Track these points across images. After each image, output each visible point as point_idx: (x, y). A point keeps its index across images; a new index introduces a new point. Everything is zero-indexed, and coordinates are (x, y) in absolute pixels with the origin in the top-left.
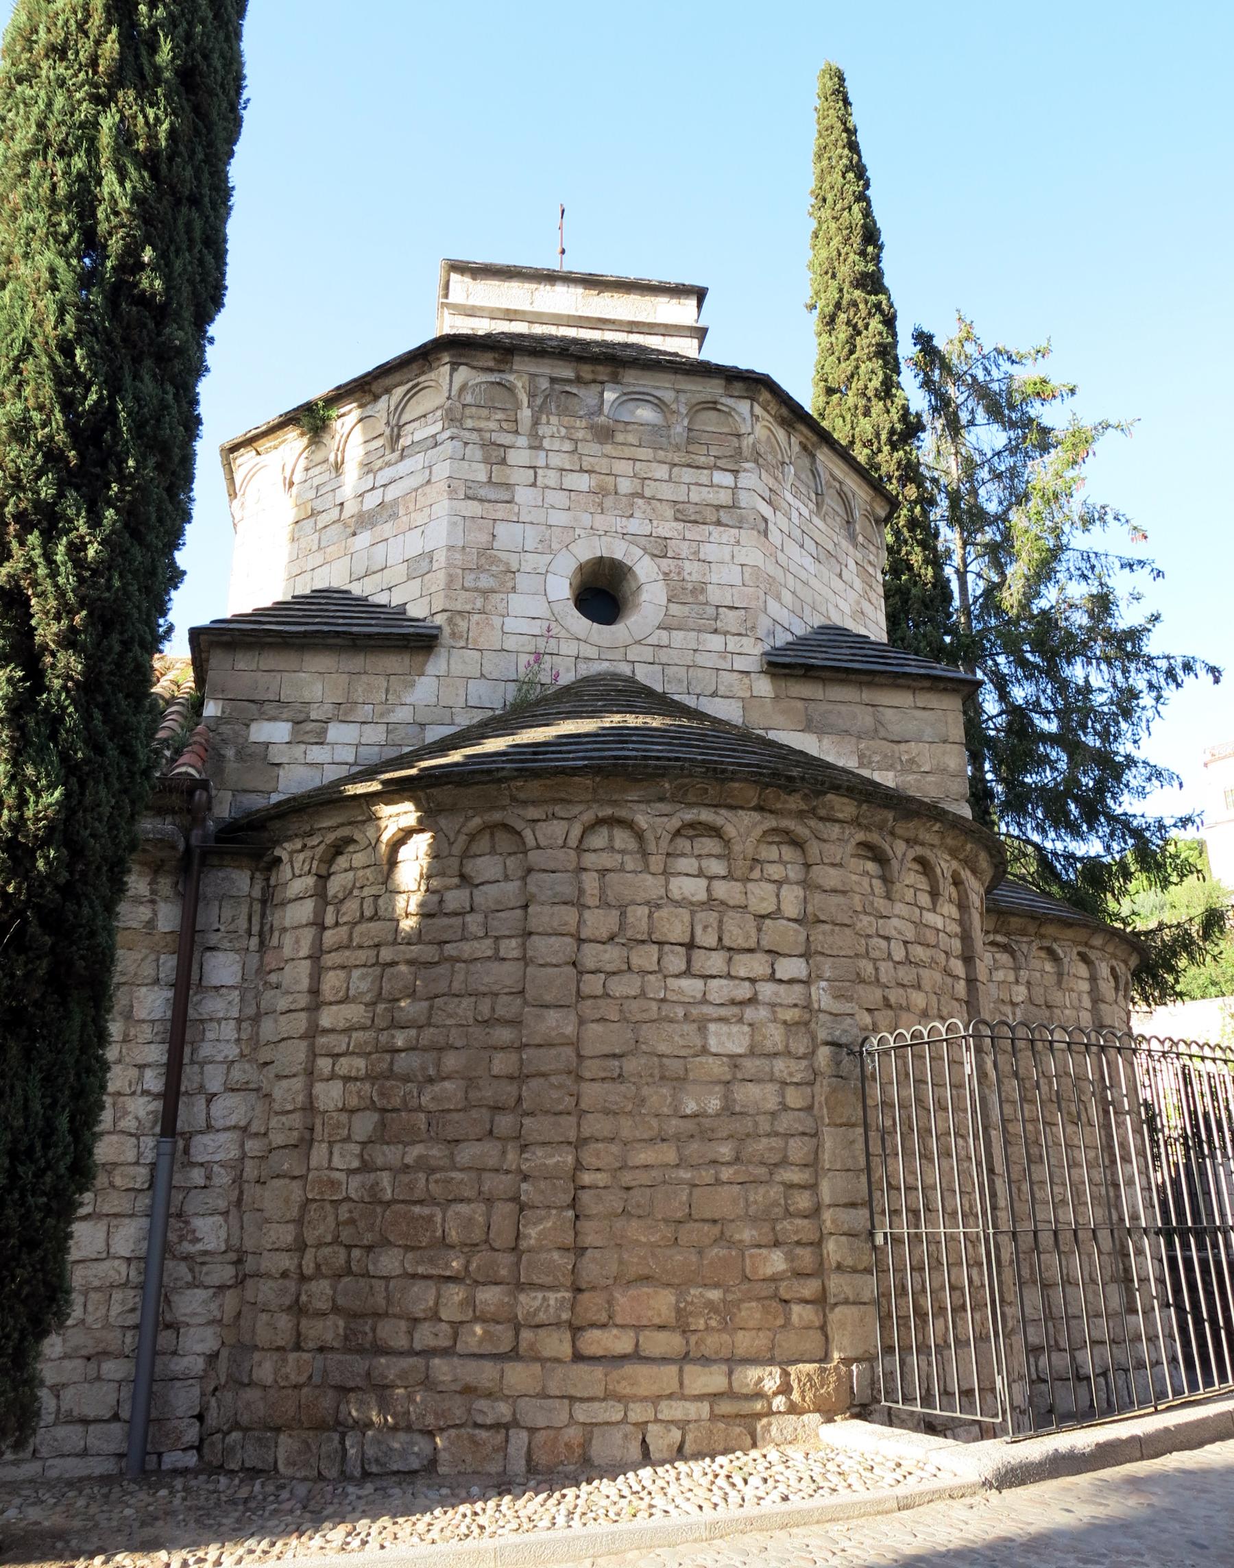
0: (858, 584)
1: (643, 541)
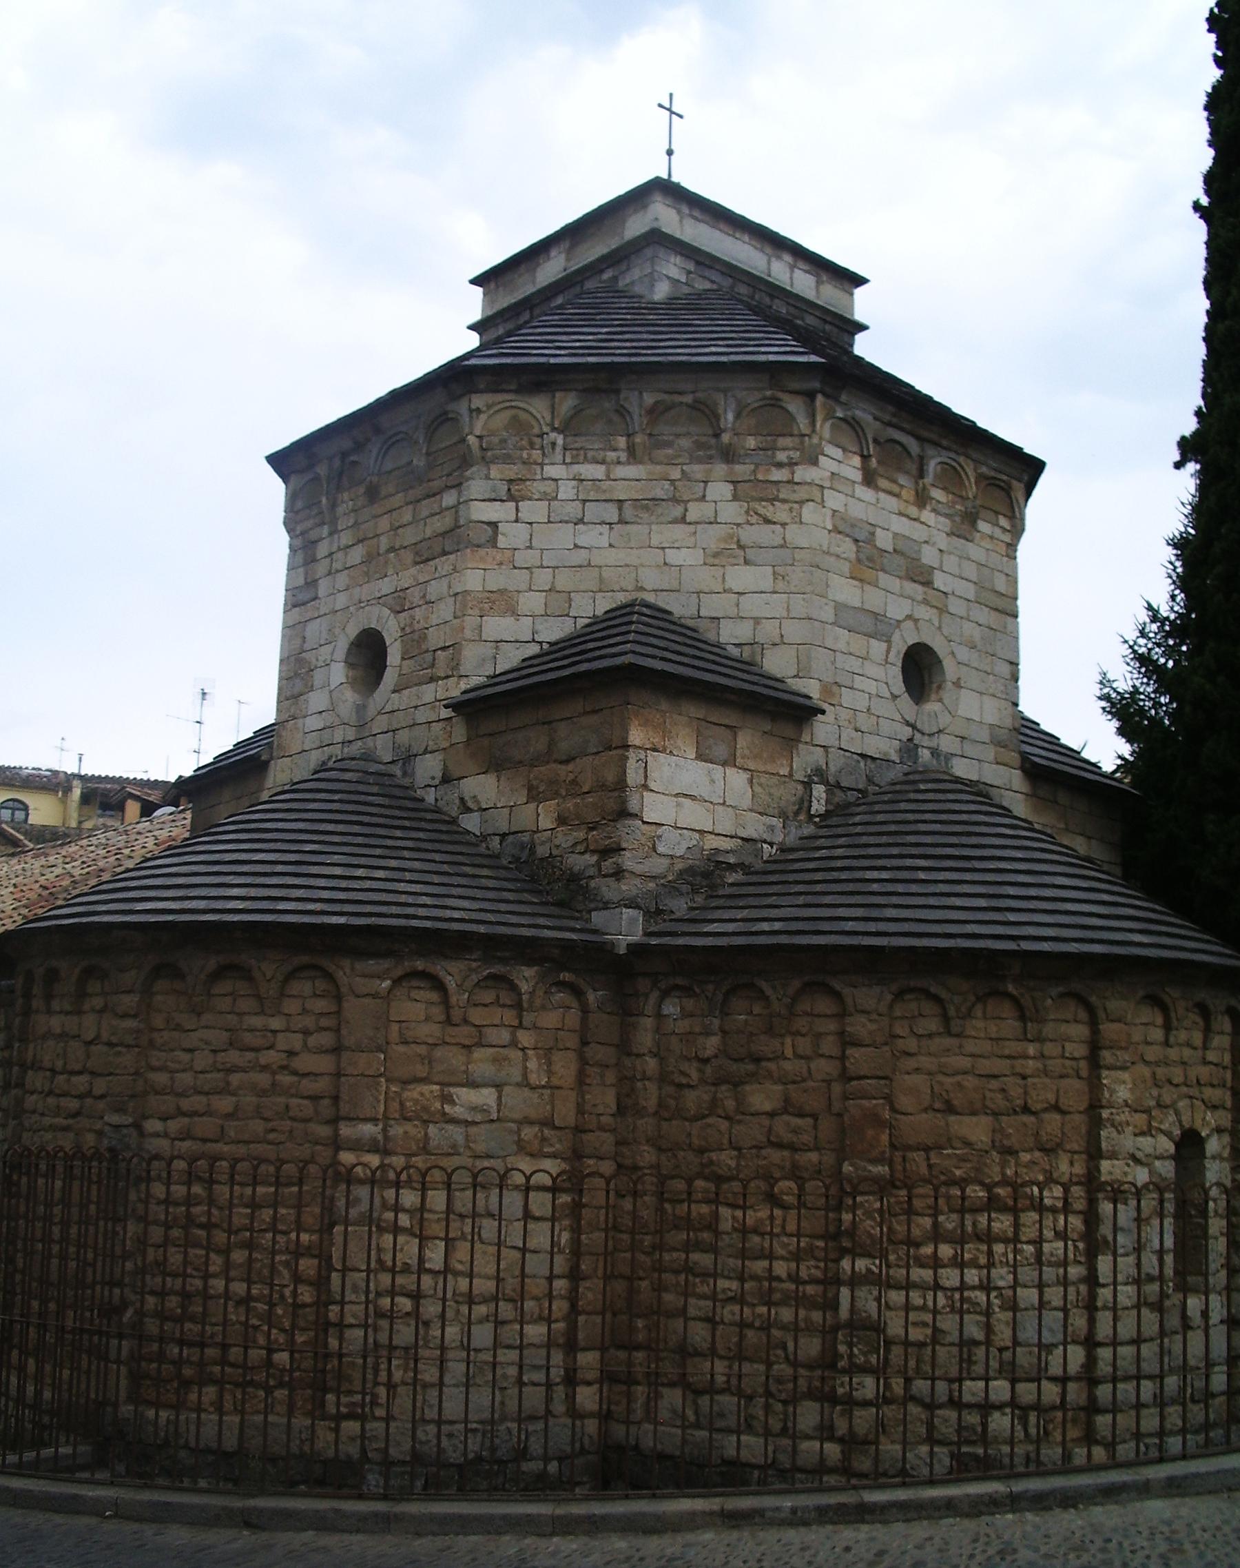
0: (731, 512)
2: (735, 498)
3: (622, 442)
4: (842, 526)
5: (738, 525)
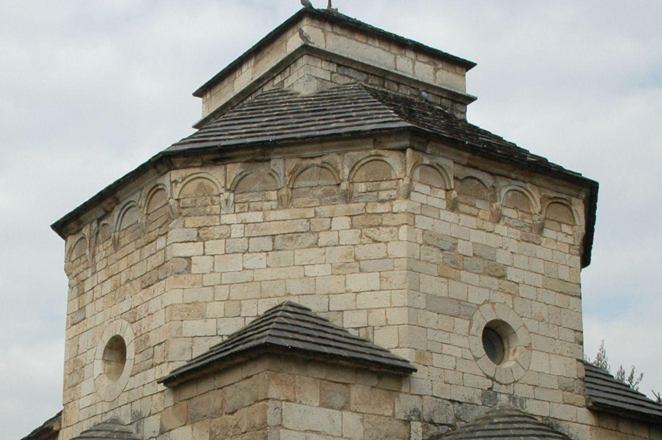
0: (349, 236)
2: (352, 227)
3: (273, 195)
4: (430, 241)
5: (354, 245)
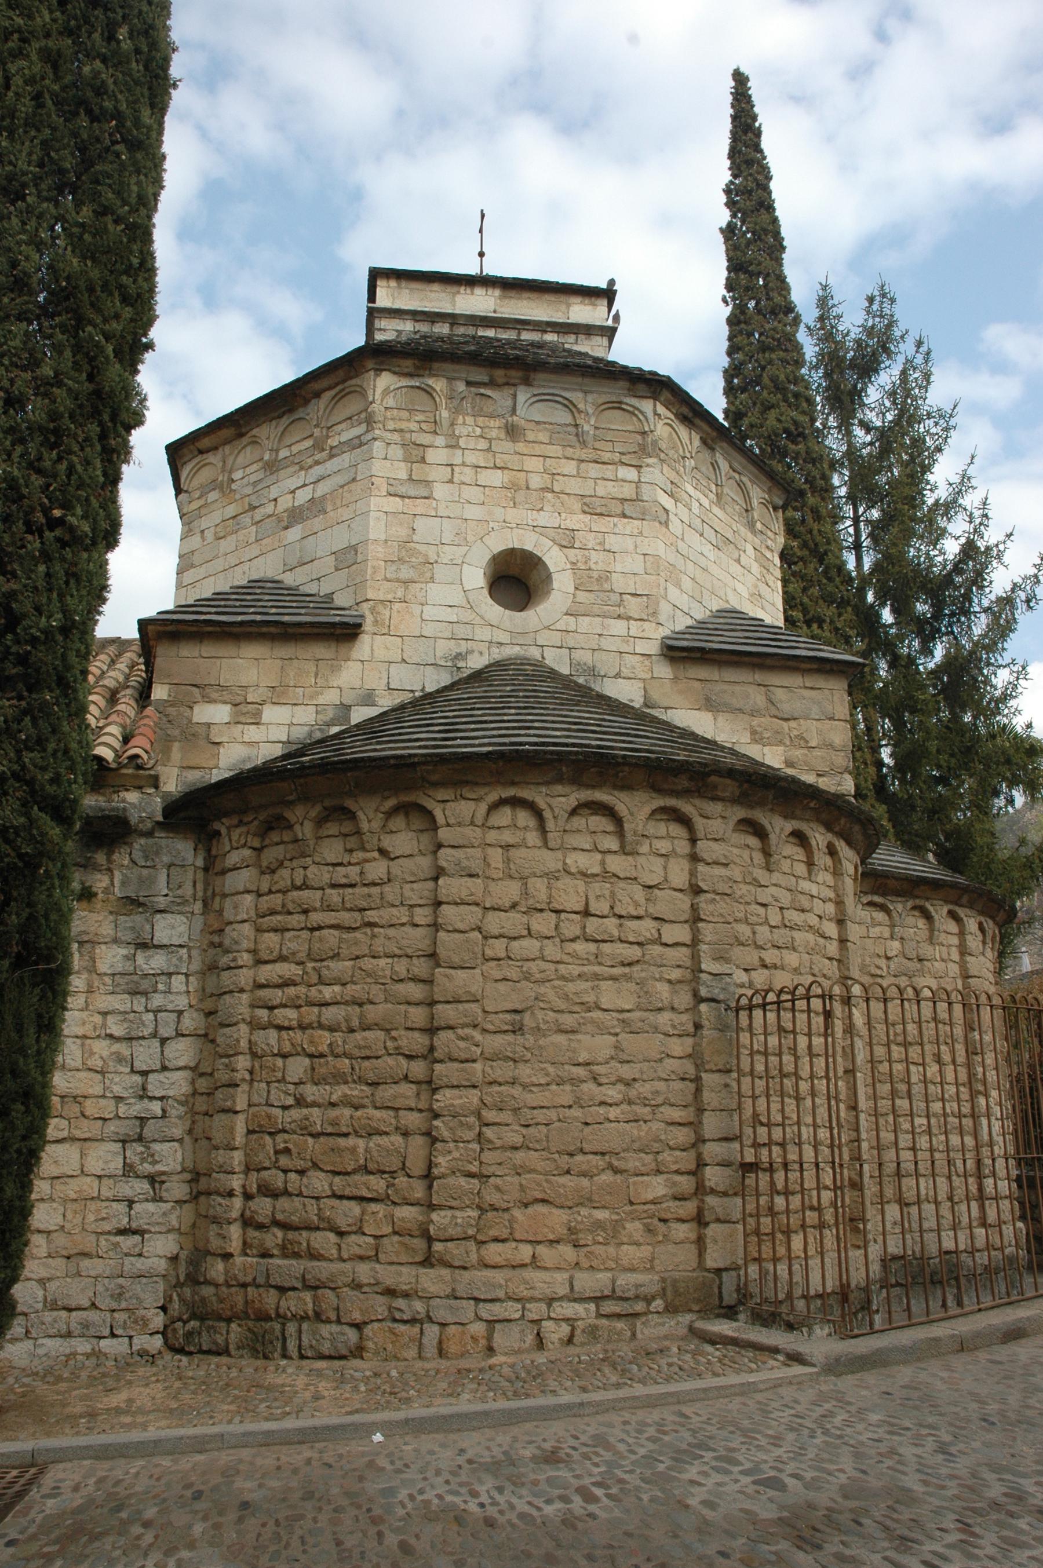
0: (755, 568)
1: (551, 533)
